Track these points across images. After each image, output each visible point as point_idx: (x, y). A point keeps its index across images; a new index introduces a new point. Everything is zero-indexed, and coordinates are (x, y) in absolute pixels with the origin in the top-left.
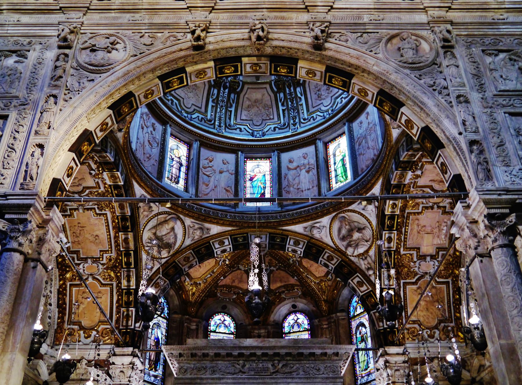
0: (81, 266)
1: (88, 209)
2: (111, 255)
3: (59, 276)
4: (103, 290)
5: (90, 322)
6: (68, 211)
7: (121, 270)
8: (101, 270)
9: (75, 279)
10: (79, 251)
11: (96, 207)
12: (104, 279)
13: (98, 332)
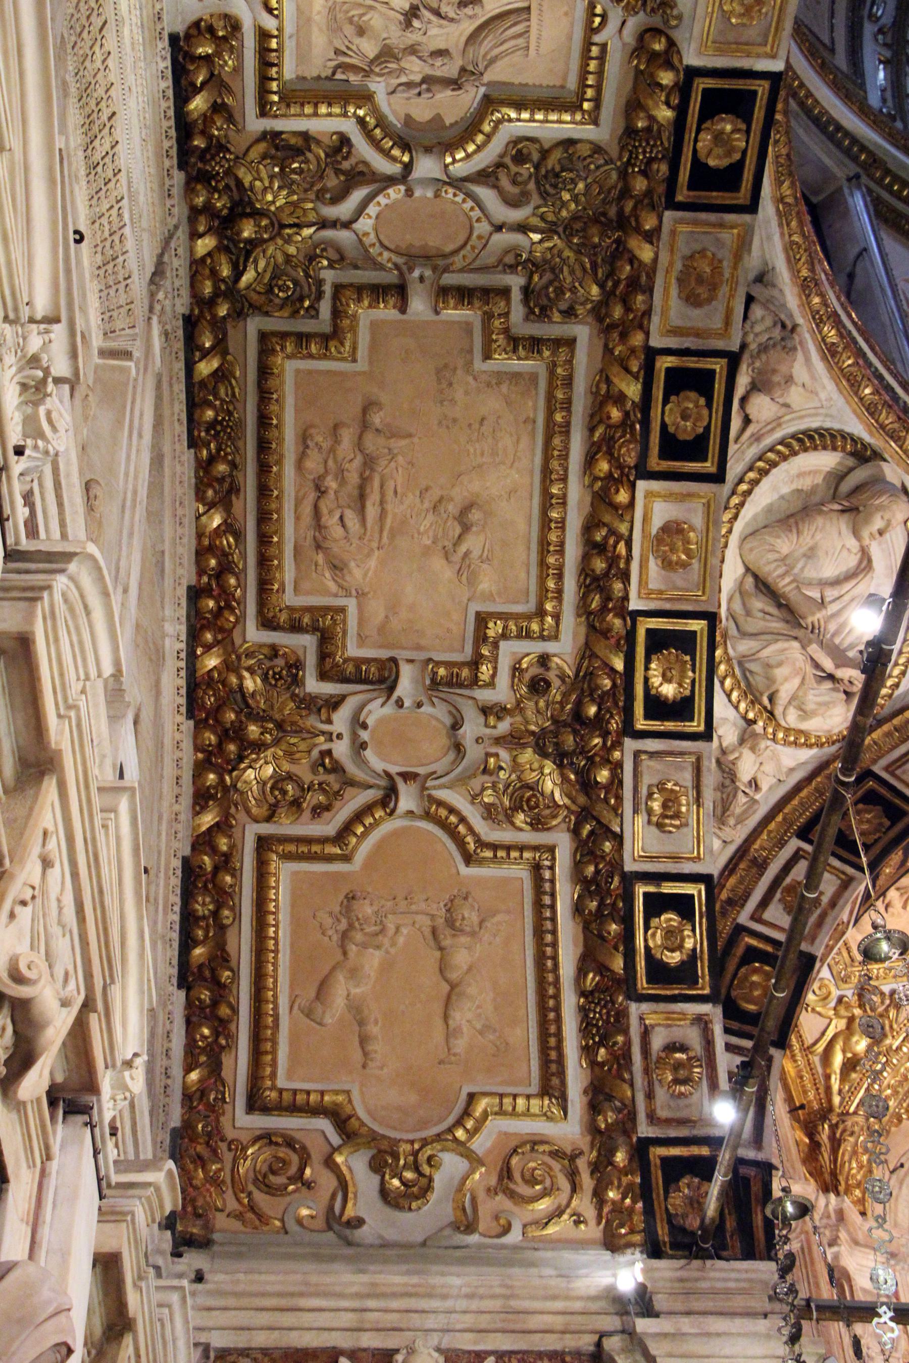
0: (341, 720)
1: (464, 295)
2: (550, 647)
3: (199, 769)
4: (480, 881)
5: (413, 1098)
6: (325, 308)
7: (617, 744)
8: (474, 752)
9: (296, 804)
10: (342, 610)
11: (516, 282)
12: (489, 812)
13: (475, 1160)
